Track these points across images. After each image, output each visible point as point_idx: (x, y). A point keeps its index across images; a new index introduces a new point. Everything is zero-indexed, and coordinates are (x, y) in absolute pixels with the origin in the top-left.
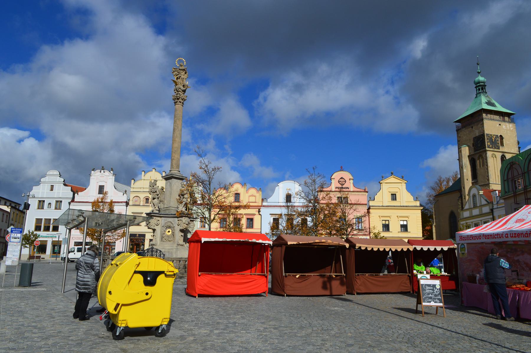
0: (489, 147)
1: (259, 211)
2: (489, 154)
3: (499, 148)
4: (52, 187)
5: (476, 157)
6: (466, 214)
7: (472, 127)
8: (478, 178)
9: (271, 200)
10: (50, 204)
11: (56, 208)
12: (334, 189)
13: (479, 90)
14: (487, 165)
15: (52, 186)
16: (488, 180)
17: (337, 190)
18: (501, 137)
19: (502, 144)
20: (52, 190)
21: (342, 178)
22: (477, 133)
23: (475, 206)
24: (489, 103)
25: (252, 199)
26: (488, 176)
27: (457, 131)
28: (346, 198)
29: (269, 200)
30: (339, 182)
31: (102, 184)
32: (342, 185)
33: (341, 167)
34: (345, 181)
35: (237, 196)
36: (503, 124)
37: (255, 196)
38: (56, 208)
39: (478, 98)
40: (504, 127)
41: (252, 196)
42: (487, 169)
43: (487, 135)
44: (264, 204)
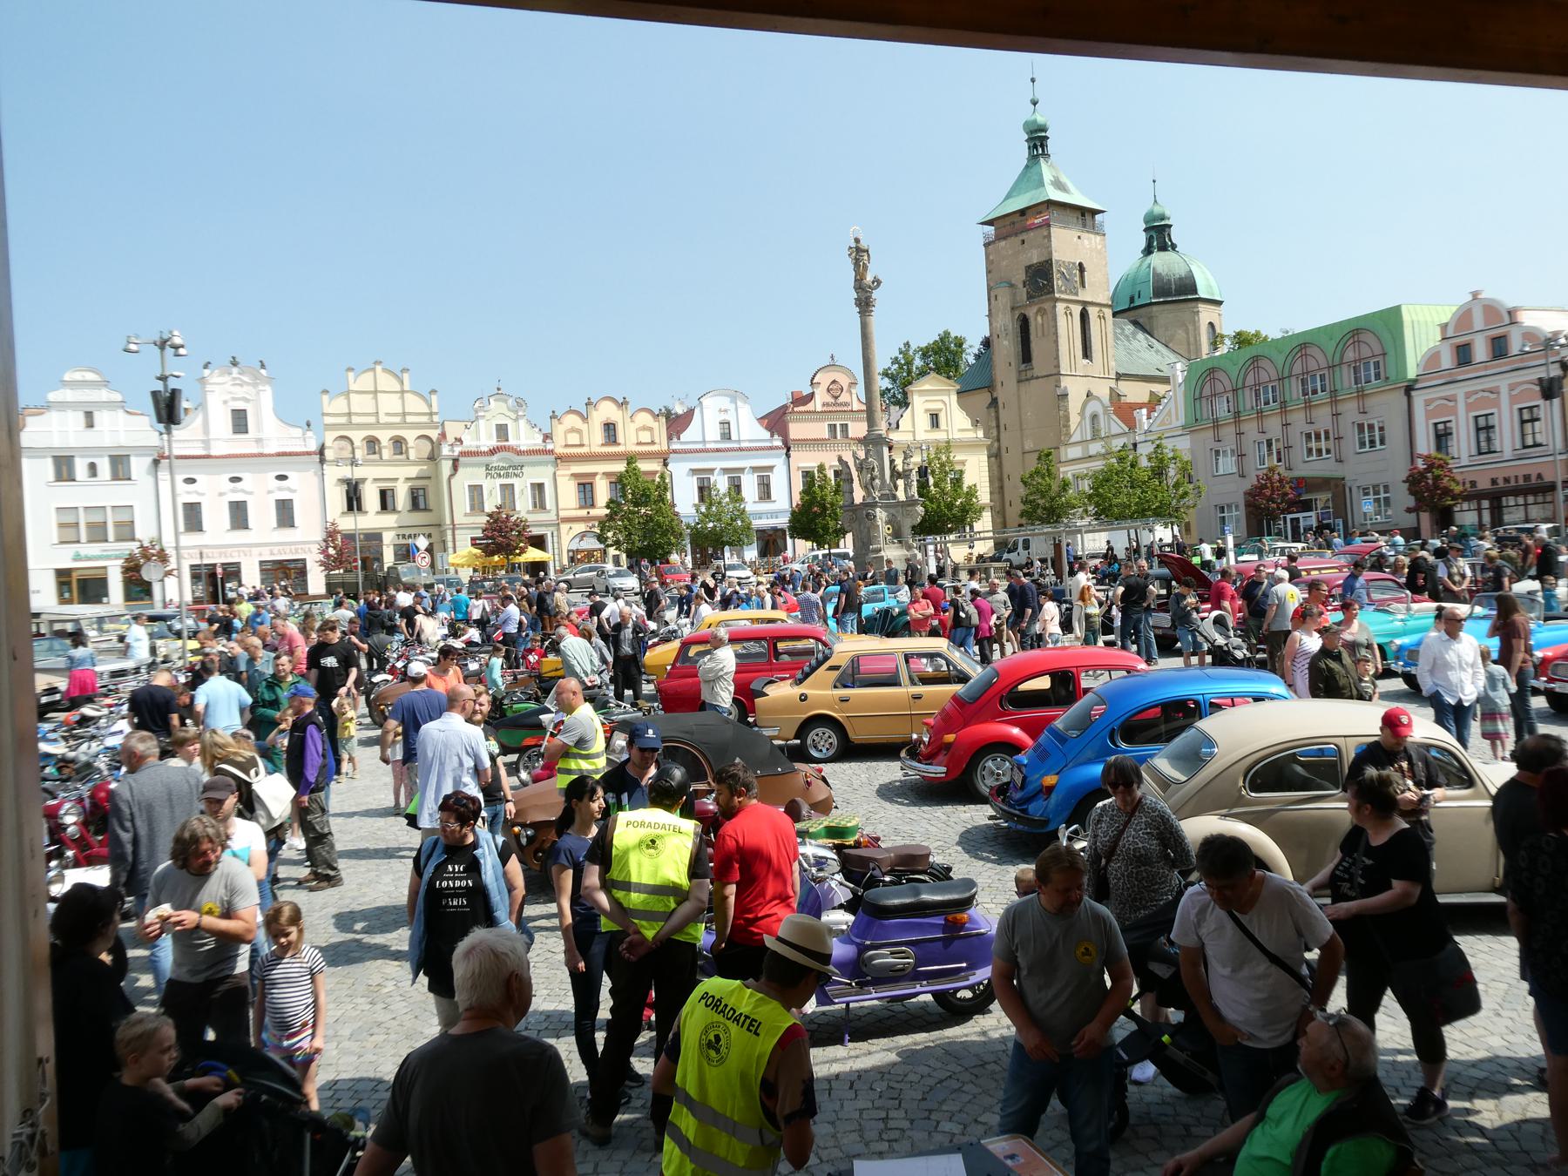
0: (1061, 292)
1: (666, 465)
2: (1060, 307)
3: (1077, 294)
4: (89, 416)
5: (1031, 313)
6: (1074, 452)
7: (1023, 242)
8: (1034, 362)
9: (691, 435)
10: (93, 468)
11: (116, 476)
12: (819, 409)
13: (1035, 147)
14: (1056, 334)
15: (89, 416)
16: (1058, 366)
17: (825, 409)
18: (1081, 268)
19: (1084, 286)
20: (90, 424)
21: (834, 382)
22: (1035, 257)
23: (1096, 436)
24: (1059, 185)
25: (645, 437)
26: (1057, 357)
27: (986, 245)
28: (845, 427)
29: (684, 437)
30: (828, 390)
31: (240, 405)
32: (836, 398)
33: (832, 357)
34: (842, 390)
35: (610, 429)
36: (1085, 235)
37: (651, 429)
38: (116, 476)
39: (1034, 170)
40: (1086, 242)
41: (644, 428)
42: (1056, 342)
43: (1057, 261)
44: (675, 446)
